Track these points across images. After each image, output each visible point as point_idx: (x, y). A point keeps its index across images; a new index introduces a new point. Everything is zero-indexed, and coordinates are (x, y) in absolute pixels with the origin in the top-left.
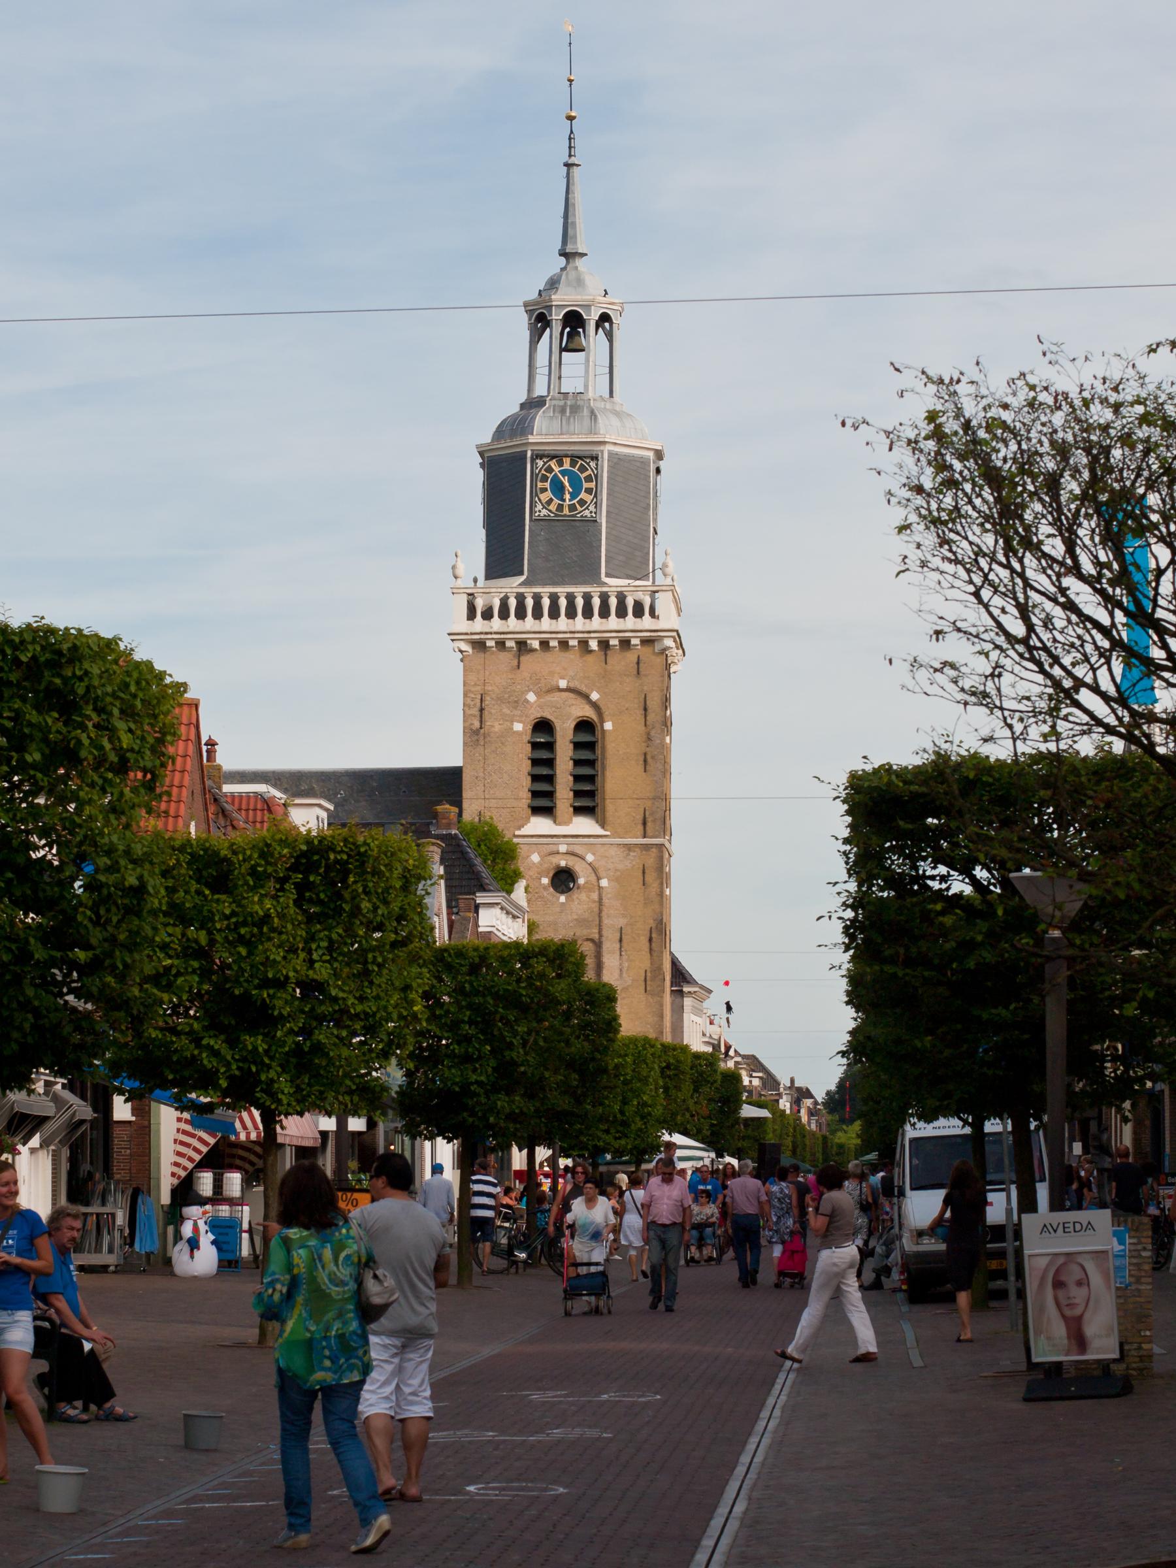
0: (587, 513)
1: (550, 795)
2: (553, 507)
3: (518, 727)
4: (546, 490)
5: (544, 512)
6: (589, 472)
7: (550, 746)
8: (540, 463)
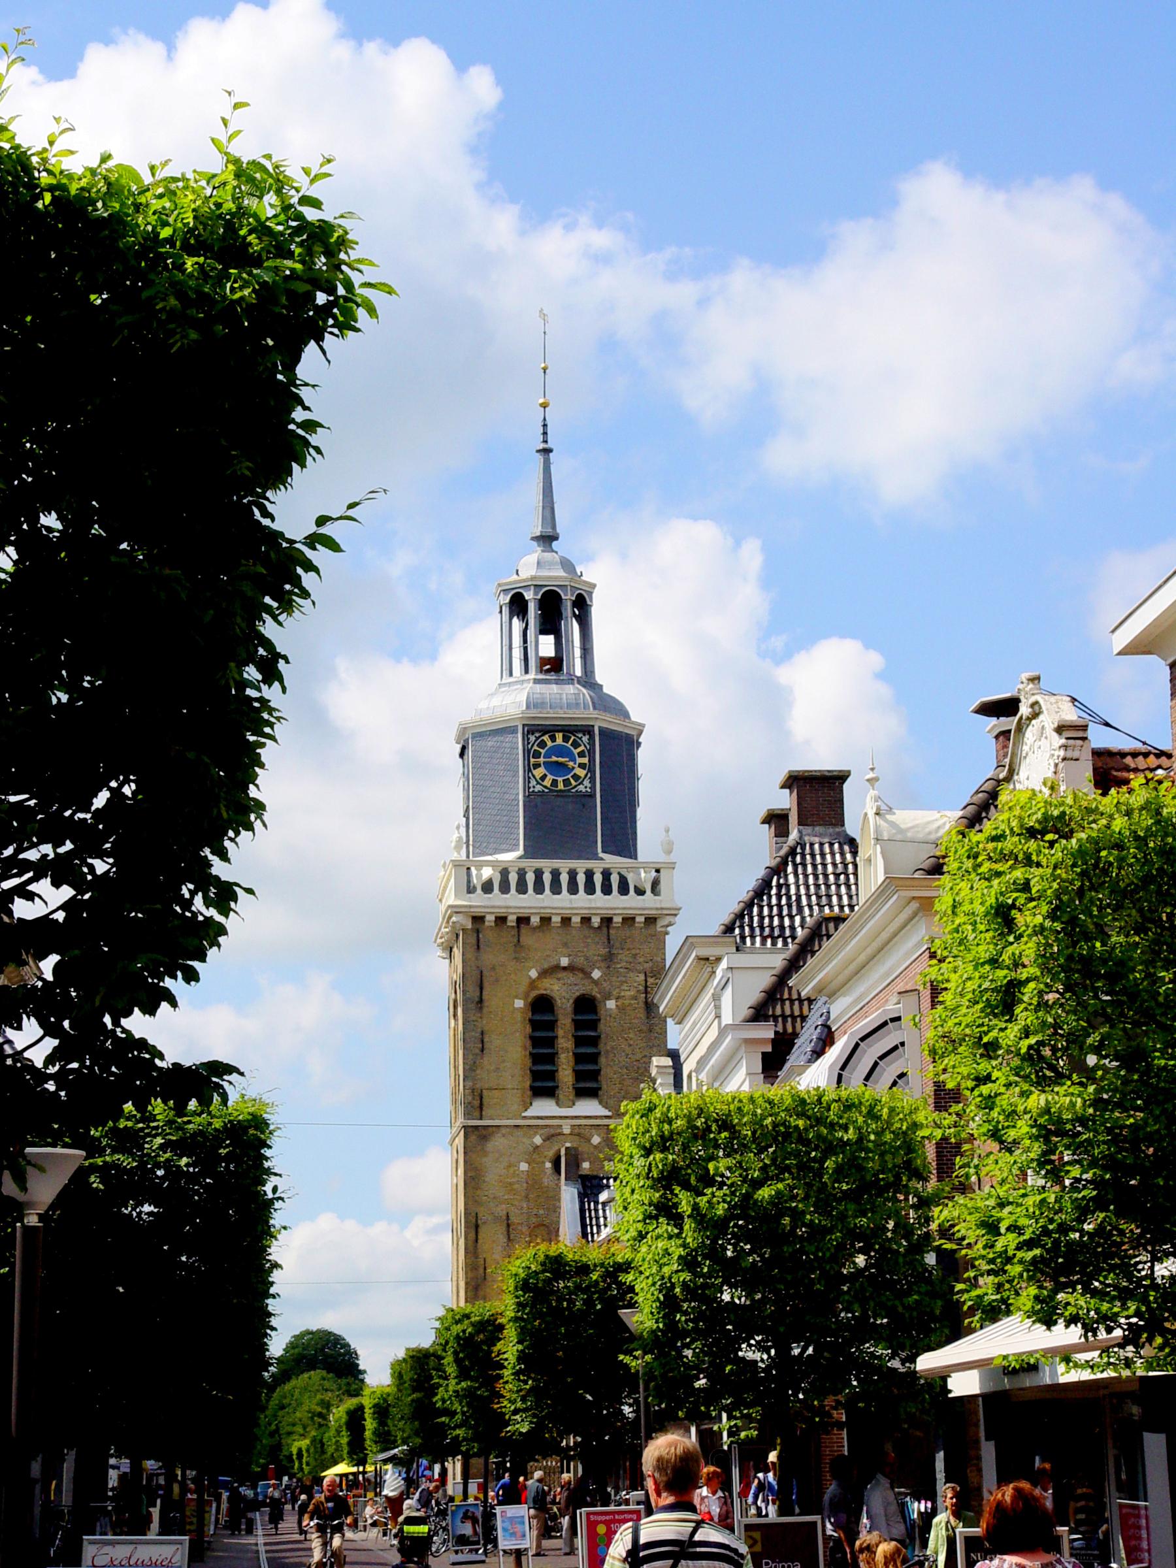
0: (581, 788)
1: (552, 1075)
2: (547, 783)
3: (519, 1003)
4: (539, 765)
5: (538, 788)
6: (582, 748)
7: (551, 1025)
8: (532, 738)
